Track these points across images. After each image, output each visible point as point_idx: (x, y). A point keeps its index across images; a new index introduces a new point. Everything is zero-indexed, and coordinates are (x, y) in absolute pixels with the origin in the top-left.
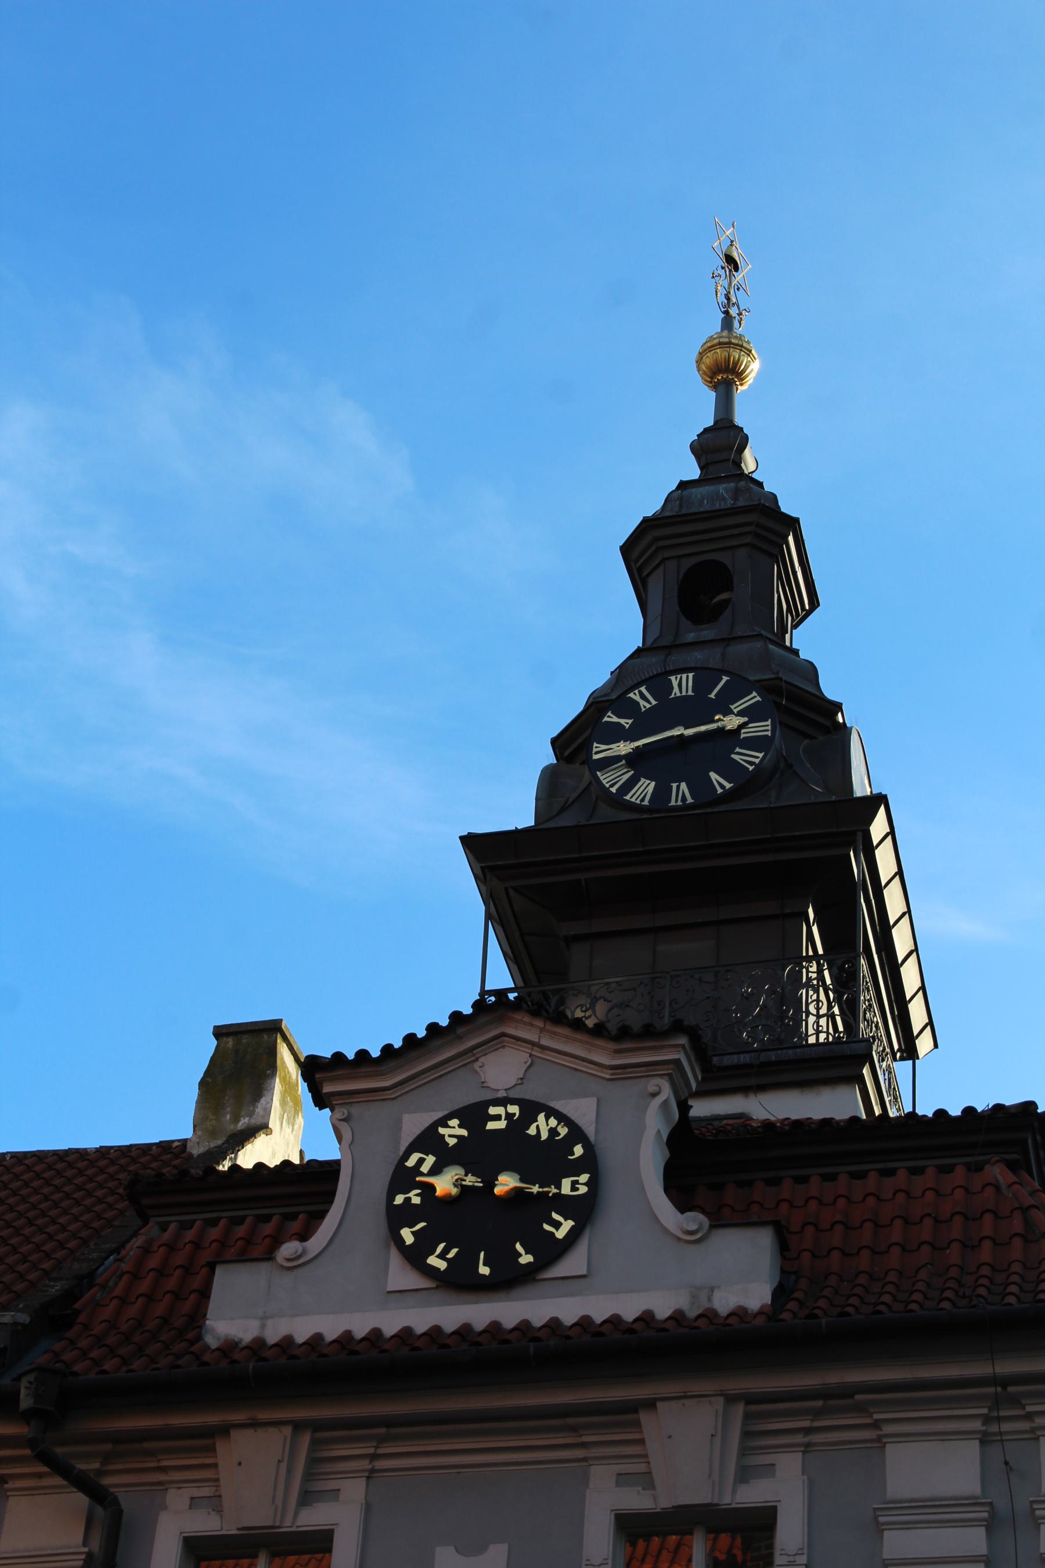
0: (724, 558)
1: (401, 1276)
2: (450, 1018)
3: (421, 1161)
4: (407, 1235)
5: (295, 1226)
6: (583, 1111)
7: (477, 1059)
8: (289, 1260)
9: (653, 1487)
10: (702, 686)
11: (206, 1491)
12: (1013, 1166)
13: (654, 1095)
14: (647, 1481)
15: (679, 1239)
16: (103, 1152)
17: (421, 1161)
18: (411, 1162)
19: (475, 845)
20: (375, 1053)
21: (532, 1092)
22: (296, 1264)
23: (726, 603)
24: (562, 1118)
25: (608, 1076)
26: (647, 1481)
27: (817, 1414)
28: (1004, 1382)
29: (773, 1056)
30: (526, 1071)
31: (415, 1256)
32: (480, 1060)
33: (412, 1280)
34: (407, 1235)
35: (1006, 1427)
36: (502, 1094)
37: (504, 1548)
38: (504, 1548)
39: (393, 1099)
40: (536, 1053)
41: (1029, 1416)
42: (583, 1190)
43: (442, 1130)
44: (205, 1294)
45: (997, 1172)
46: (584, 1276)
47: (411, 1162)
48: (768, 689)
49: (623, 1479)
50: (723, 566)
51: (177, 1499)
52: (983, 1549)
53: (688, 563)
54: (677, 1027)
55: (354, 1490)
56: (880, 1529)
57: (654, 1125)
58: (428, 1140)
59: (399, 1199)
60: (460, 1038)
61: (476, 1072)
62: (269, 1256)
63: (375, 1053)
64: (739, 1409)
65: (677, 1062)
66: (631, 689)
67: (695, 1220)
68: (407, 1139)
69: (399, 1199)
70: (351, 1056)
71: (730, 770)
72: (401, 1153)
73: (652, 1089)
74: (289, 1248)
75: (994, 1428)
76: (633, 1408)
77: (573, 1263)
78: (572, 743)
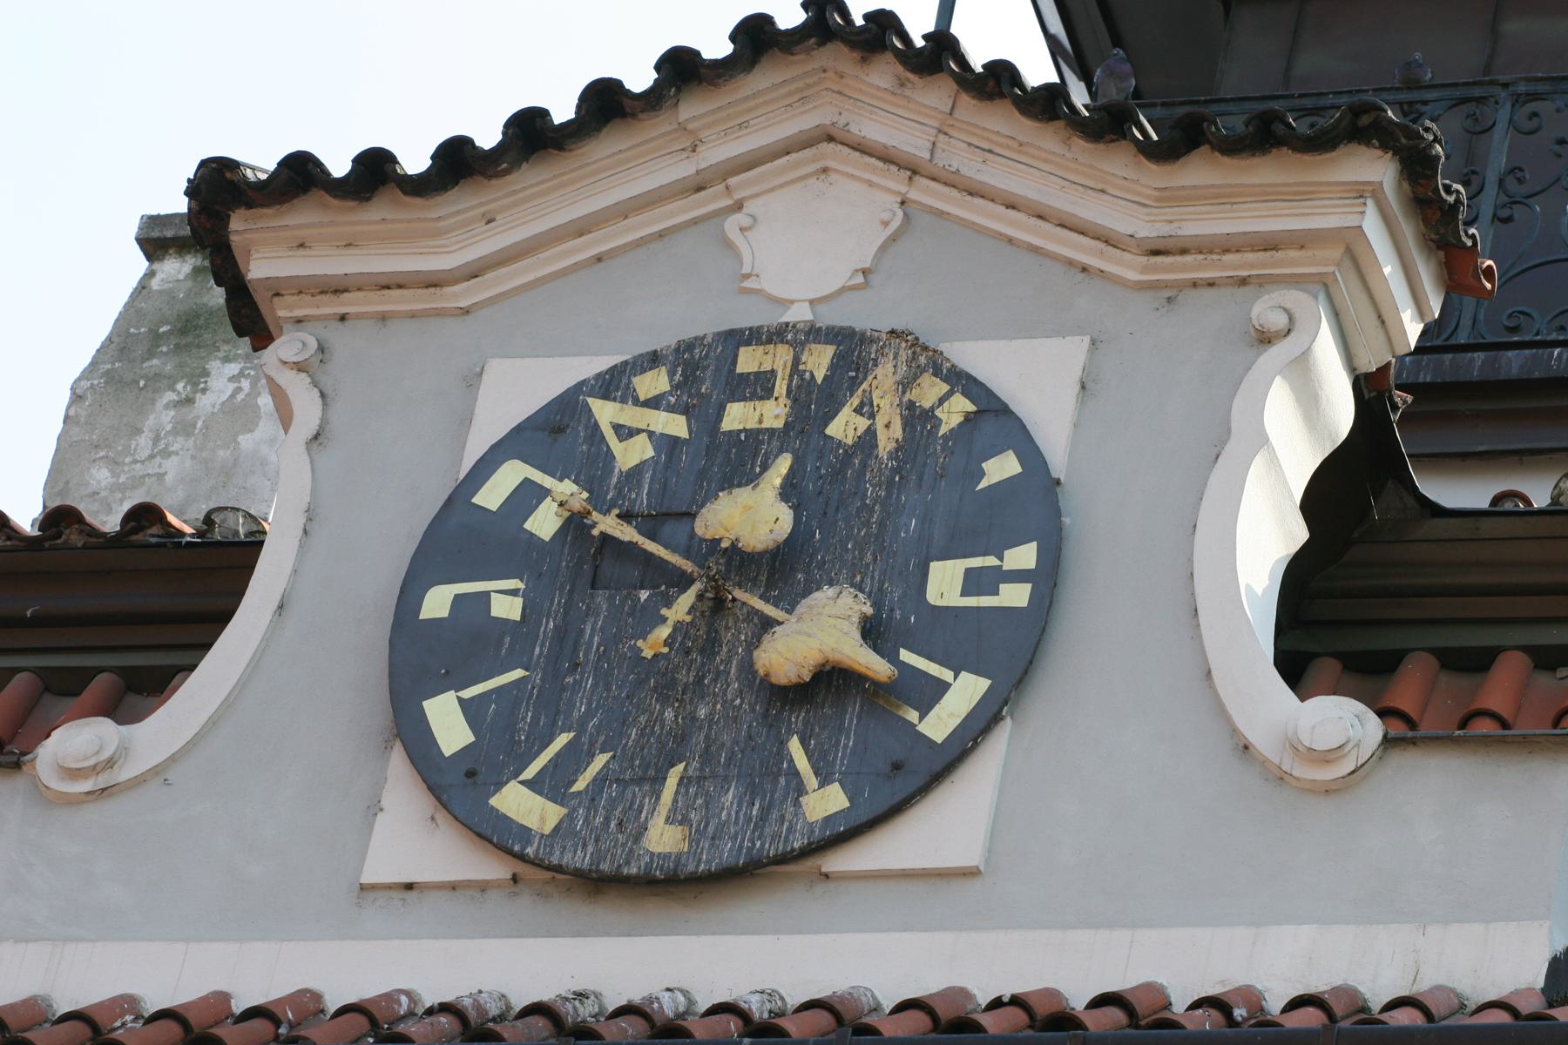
1: (409, 839)
2: (658, 67)
6: (1038, 378)
7: (738, 206)
8: (74, 774)
13: (1265, 339)
15: (1282, 778)
20: (415, 160)
25: (1132, 276)
30: (884, 248)
32: (750, 207)
33: (443, 855)
36: (799, 314)
39: (466, 311)
40: (924, 193)
46: (970, 873)
61: (728, 245)
63: (415, 160)
67: (1341, 720)
70: (339, 167)
72: (462, 476)
74: (76, 741)
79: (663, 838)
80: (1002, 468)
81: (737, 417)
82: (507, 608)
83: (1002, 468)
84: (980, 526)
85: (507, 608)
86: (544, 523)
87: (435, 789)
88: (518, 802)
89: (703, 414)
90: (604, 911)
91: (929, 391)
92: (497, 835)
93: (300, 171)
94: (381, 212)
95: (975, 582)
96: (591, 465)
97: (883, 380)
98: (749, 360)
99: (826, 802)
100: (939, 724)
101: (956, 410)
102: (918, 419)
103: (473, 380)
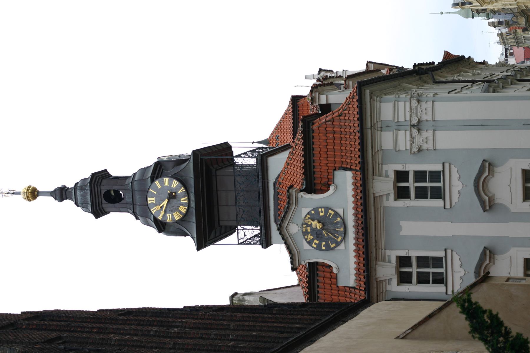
0: (103, 192)
1: (342, 247)
3: (315, 244)
4: (332, 246)
6: (305, 211)
9: (389, 194)
10: (153, 195)
11: (387, 281)
12: (313, 124)
14: (388, 195)
17: (315, 244)
18: (315, 246)
19: (199, 248)
23: (115, 191)
24: (306, 216)
26: (388, 195)
27: (376, 162)
28: (372, 126)
31: (338, 244)
33: (343, 245)
35: (379, 126)
36: (300, 228)
37: (401, 222)
38: (401, 222)
41: (377, 122)
42: (323, 209)
43: (308, 240)
45: (315, 127)
47: (315, 246)
48: (153, 179)
49: (388, 199)
50: (105, 192)
51: (388, 288)
52: (404, 131)
53: (104, 201)
55: (388, 253)
57: (308, 196)
58: (310, 243)
59: (324, 248)
60: (287, 238)
62: (336, 274)
64: (375, 177)
65: (295, 191)
66: (152, 213)
69: (324, 248)
71: (178, 188)
73: (300, 197)
74: (335, 271)
75: (379, 129)
76: (374, 197)
77: (340, 211)
78: (162, 227)
79: (342, 229)
80: (313, 212)
81: (309, 231)
82: (324, 243)
83: (313, 212)
84: (317, 213)
85: (324, 243)
86: (317, 242)
87: (338, 245)
88: (339, 240)
89: (309, 233)
90: (347, 232)
91: (307, 218)
92: (341, 241)
93: (292, 263)
94: (294, 258)
95: (322, 212)
96: (313, 240)
97: (306, 221)
98: (304, 231)
99: (339, 219)
100: (332, 213)
101: (309, 216)
102: (309, 218)
103: (305, 250)
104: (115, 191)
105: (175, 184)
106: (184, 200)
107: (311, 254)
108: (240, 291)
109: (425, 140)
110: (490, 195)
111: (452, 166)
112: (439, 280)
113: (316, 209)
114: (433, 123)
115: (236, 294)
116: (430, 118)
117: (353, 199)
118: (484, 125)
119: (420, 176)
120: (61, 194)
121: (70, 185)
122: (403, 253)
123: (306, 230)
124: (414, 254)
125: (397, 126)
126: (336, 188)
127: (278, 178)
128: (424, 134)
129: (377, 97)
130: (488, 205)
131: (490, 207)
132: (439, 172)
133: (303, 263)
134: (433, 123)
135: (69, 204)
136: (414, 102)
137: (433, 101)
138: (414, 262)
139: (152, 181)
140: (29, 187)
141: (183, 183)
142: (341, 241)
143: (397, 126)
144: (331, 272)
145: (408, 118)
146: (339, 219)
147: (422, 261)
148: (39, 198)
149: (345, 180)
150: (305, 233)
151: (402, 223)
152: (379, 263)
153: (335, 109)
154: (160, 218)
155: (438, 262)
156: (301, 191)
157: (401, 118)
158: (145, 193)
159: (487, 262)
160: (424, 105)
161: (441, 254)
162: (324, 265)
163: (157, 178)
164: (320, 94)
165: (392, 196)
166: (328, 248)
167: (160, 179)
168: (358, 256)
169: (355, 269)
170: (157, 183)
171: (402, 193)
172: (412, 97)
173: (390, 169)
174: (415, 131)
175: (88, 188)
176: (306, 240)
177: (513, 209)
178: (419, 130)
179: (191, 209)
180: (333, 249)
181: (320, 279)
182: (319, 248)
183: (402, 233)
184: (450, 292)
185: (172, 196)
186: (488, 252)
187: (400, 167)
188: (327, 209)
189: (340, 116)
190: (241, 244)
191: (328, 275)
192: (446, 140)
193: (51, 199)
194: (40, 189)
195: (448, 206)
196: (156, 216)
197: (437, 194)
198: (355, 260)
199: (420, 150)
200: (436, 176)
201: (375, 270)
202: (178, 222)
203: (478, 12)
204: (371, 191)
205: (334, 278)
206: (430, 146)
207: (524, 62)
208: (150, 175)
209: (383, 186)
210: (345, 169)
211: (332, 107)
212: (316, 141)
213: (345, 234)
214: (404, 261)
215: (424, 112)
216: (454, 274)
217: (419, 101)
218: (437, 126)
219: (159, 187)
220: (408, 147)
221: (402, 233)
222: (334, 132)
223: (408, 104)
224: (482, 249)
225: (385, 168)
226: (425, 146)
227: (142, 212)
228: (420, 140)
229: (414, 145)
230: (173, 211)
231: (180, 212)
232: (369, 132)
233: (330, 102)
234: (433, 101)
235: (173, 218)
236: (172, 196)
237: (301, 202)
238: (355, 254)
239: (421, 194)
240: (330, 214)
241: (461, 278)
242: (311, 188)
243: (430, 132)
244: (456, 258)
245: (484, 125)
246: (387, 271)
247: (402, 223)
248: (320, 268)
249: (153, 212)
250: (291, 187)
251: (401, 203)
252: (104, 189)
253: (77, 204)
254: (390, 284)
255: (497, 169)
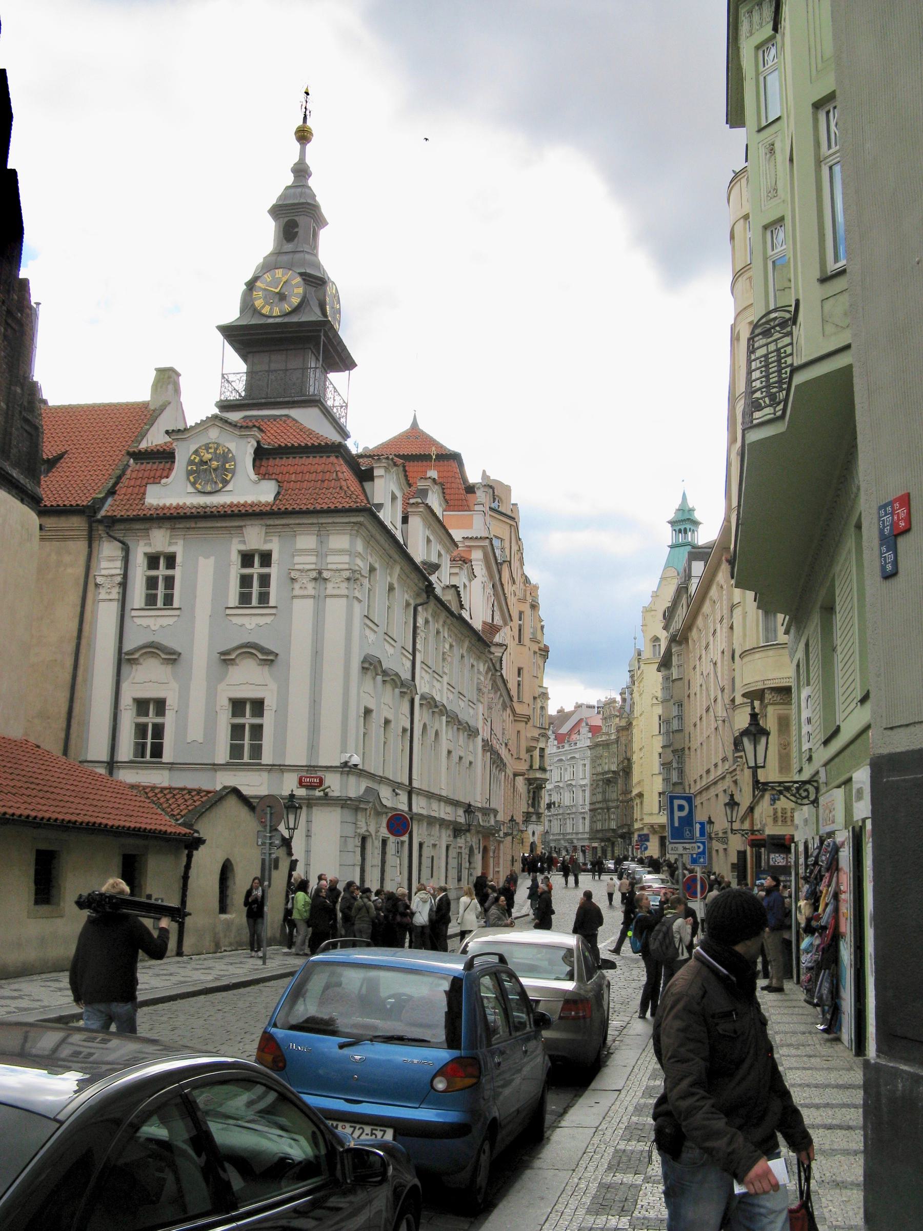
5: (165, 474)
12: (337, 457)
16: (127, 404)
21: (220, 442)
22: (166, 485)
26: (244, 542)
29: (296, 399)
31: (193, 484)
34: (192, 480)
44: (144, 494)
45: (333, 459)
51: (142, 543)
53: (286, 219)
54: (254, 426)
55: (181, 542)
56: (294, 556)
58: (196, 452)
68: (191, 452)
74: (164, 481)
76: (241, 527)
77: (229, 487)
79: (209, 489)
86: (196, 461)
92: (196, 489)
93: (173, 431)
96: (199, 455)
99: (221, 485)
104: (297, 232)
105: (295, 301)
106: (276, 311)
107: (183, 454)
108: (182, 380)
109: (303, 586)
110: (237, 661)
111: (272, 617)
112: (151, 600)
113: (233, 457)
114: (322, 595)
115: (179, 375)
116: (329, 592)
117: (242, 502)
118: (317, 654)
119: (265, 580)
120: (301, 171)
121: (311, 182)
122: (179, 559)
123: (211, 448)
124: (178, 573)
125: (320, 554)
126: (256, 483)
127: (294, 420)
128: (310, 586)
129: (357, 531)
130: (226, 659)
131: (224, 660)
132: (268, 603)
133: (174, 444)
134: (322, 595)
135: (289, 179)
136: (347, 574)
137: (347, 596)
138: (169, 572)
139: (301, 274)
140: (312, 134)
141: (296, 310)
142: (196, 489)
143: (320, 554)
144: (161, 477)
145: (330, 567)
146: (221, 485)
147: (170, 582)
148: (297, 146)
149: (264, 493)
150: (207, 447)
151: (212, 560)
152: (169, 531)
153: (367, 485)
154: (258, 284)
155: (169, 600)
156: (258, 442)
157: (330, 559)
158: (289, 267)
159: (164, 656)
160: (345, 585)
161: (175, 605)
162: (171, 469)
163: (304, 280)
164: (387, 469)
165: (243, 547)
166: (189, 473)
167: (302, 282)
168: (178, 507)
169: (165, 505)
170: (299, 279)
171: (247, 559)
172: (354, 571)
173: (274, 546)
174: (314, 574)
175: (302, 201)
176: (200, 447)
177: (221, 687)
178: (315, 579)
179: (265, 319)
180: (188, 479)
181: (161, 466)
182: (191, 462)
183: (201, 560)
184: (134, 613)
185: (282, 297)
186: (174, 657)
187: (275, 557)
188: (233, 472)
189: (341, 488)
190: (223, 377)
191: (158, 474)
192: (303, 610)
193: (296, 159)
194: (309, 147)
195: (229, 612)
196: (261, 279)
197: (245, 599)
198: (174, 504)
199: (293, 580)
200: (264, 598)
201: (160, 527)
202: (253, 305)
203: (632, 677)
204: (249, 523)
205: (156, 480)
206: (297, 592)
207: (587, 724)
208: (308, 271)
209: (254, 537)
210: (278, 493)
211: (370, 483)
212: (317, 460)
213: (204, 493)
214: (171, 561)
215: (336, 586)
216: (152, 619)
217: (348, 579)
218: (319, 599)
219: (293, 282)
220: (297, 567)
221: (201, 560)
222: (323, 481)
223: (346, 566)
224: (179, 650)
225: (276, 539)
226: (297, 586)
227: (269, 265)
228: (304, 580)
229: (298, 573)
230: (265, 298)
231: (263, 307)
232: (315, 521)
233: (376, 480)
234: (347, 596)
235: (256, 299)
236: (282, 297)
237: (243, 442)
238: (181, 504)
239: (245, 581)
240: (227, 476)
241: (148, 626)
242: (261, 454)
243: (310, 591)
244: (171, 621)
245: (317, 654)
246: (159, 540)
247: (212, 559)
248: (168, 466)
249: (265, 276)
250: (261, 430)
251: (236, 559)
252: (301, 220)
253: (287, 188)
254: (145, 545)
255: (266, 668)
